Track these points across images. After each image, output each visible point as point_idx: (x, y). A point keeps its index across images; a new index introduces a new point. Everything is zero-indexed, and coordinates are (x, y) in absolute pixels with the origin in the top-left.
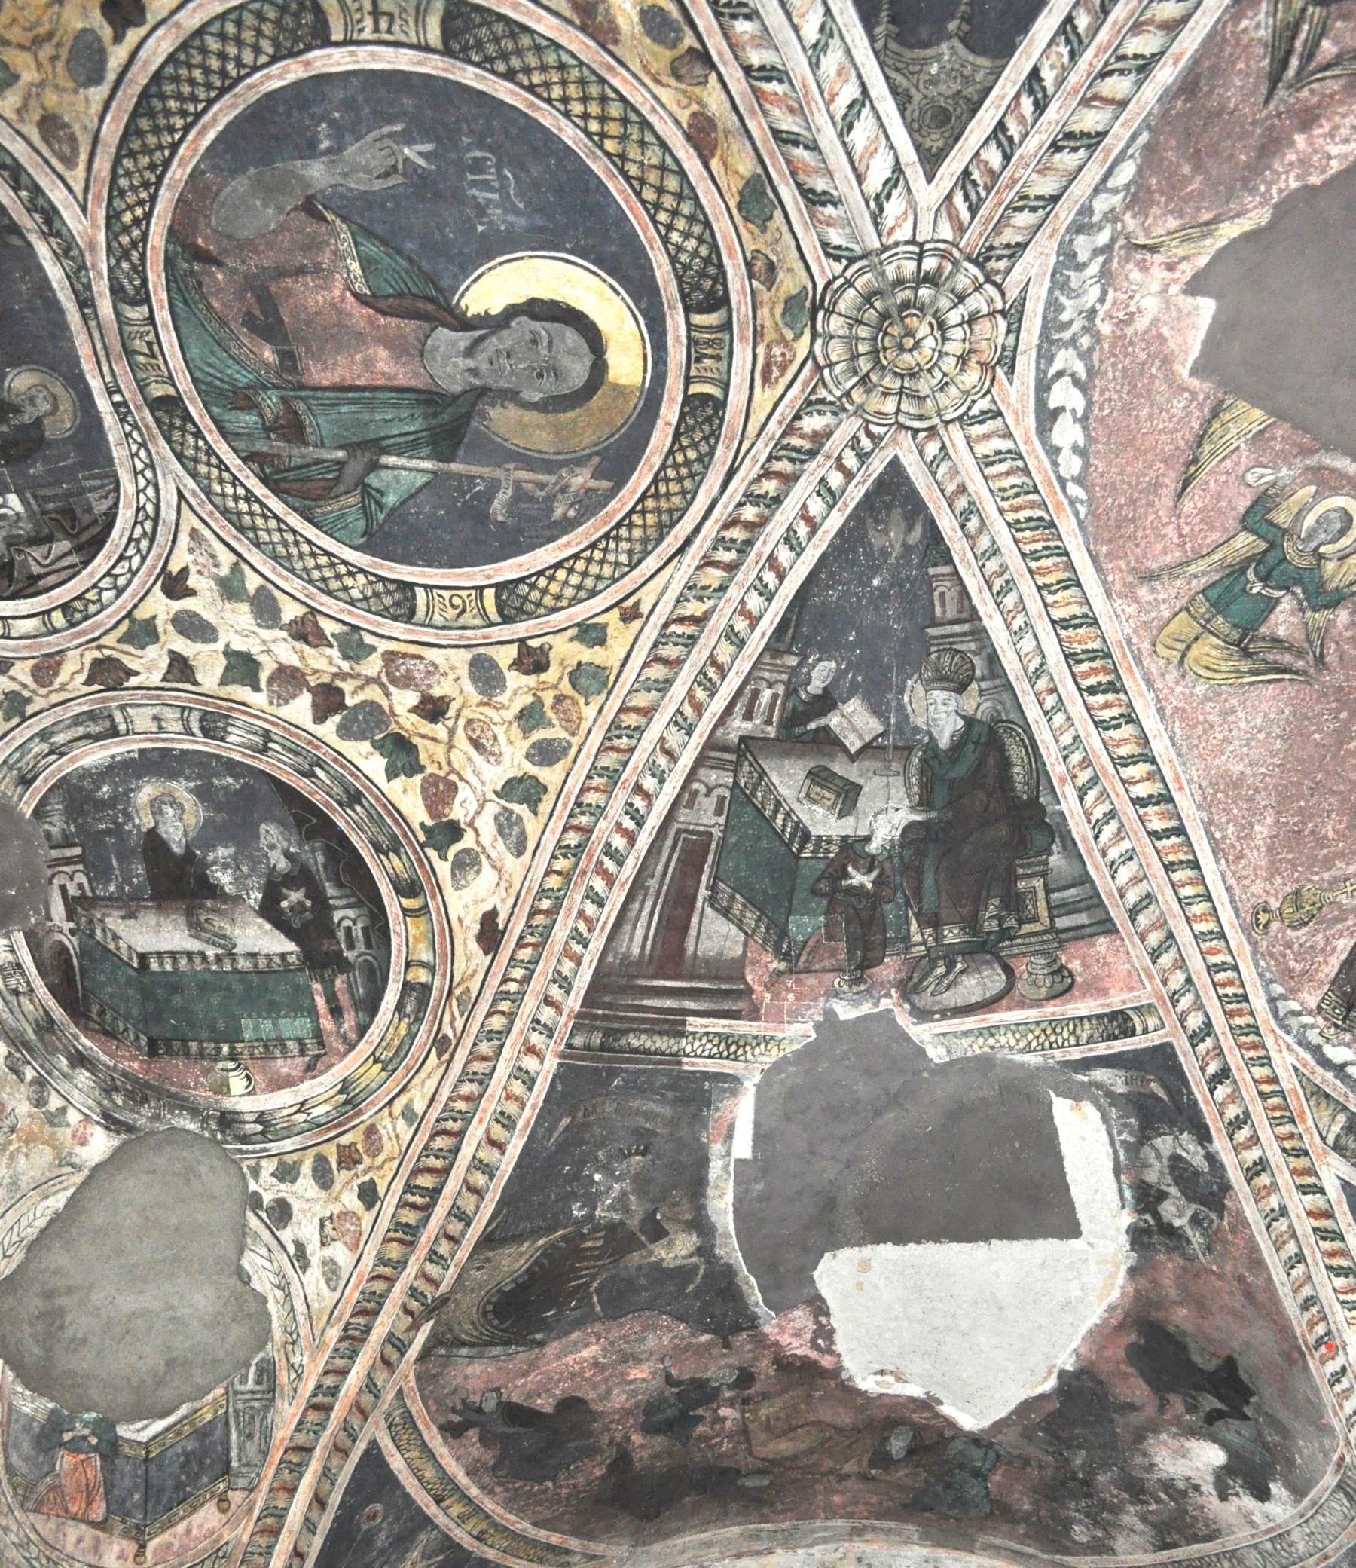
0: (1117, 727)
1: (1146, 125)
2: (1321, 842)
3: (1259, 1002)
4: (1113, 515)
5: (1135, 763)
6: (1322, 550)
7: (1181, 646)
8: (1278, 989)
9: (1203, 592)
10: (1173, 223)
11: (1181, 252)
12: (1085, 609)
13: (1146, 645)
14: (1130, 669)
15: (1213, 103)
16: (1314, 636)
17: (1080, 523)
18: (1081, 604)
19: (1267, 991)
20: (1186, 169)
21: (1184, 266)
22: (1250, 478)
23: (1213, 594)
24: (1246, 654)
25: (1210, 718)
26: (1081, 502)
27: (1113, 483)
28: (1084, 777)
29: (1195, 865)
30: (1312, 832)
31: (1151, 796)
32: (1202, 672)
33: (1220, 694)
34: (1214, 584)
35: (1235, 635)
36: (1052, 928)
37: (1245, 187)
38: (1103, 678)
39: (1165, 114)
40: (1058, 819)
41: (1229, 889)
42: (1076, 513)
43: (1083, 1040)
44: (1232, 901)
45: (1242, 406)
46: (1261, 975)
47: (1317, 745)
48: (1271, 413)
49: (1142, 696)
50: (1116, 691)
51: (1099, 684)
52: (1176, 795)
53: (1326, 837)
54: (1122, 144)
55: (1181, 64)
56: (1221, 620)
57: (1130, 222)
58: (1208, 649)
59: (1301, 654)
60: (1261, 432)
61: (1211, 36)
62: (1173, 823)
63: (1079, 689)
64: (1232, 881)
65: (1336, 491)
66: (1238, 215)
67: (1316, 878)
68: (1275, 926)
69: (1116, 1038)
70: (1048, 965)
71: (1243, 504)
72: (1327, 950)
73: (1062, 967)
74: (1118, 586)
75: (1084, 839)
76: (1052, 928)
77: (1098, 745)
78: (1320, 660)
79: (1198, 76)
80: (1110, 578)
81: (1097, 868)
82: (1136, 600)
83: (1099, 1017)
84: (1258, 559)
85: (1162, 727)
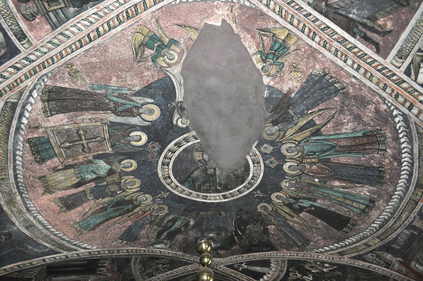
0: (118, 20)
1: (256, 7)
2: (93, 73)
3: (44, 71)
4: (172, 10)
5: (108, 26)
6: (166, 56)
7: (140, 31)
8: (50, 75)
9: (155, 34)
10: (236, 15)
11: (231, 17)
12: (148, 7)
13: (140, 23)
14: (134, 20)
15: (258, 19)
16: (145, 59)
17: (170, 3)
18: (150, 6)
19: (48, 73)
20: (246, 16)
21: (228, 18)
22: (181, 39)
23: (154, 36)
24: (140, 46)
25: (123, 42)
26: (176, 3)
27: (180, 9)
28: (101, 13)
29: (81, 46)
30: (96, 71)
31: (99, 32)
32: (134, 37)
33: (129, 42)
34: (156, 36)
35: (144, 43)
36: (48, 12)
37: (242, 27)
38: (131, 14)
39: (258, 10)
40: (85, 8)
41: (76, 56)
42: (173, 2)
43: (11, 27)
44: (73, 58)
45: (197, 34)
46: (53, 70)
47: (119, 66)
48: (196, 40)
49: (127, 25)
50: (127, 18)
51: (129, 14)
52: (101, 38)
53: (95, 74)
54: (253, 2)
55: (266, 12)
56: (148, 39)
57: (237, 6)
58: (140, 38)
59: (141, 57)
60: (192, 39)
61: (271, 17)
62: (92, 39)
63: (127, 9)
64: (78, 56)
65: (179, 56)
66: (237, 27)
67: (84, 75)
68: (68, 69)
69: (16, 37)
70: (34, 12)
71: (175, 38)
72: (64, 82)
73: (35, 17)
74: (155, 14)
75: (81, 17)
76: (48, 12)
77: (112, 17)
78: (140, 61)
79: (263, 16)
80: (157, 12)
81: (73, 21)
82: (151, 19)
83: (21, 30)
84: (163, 44)
85: (119, 31)
